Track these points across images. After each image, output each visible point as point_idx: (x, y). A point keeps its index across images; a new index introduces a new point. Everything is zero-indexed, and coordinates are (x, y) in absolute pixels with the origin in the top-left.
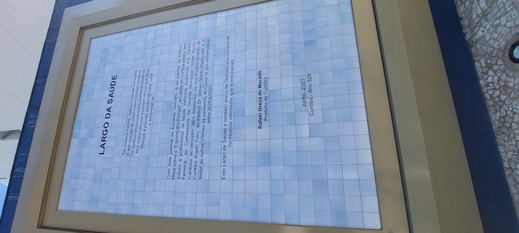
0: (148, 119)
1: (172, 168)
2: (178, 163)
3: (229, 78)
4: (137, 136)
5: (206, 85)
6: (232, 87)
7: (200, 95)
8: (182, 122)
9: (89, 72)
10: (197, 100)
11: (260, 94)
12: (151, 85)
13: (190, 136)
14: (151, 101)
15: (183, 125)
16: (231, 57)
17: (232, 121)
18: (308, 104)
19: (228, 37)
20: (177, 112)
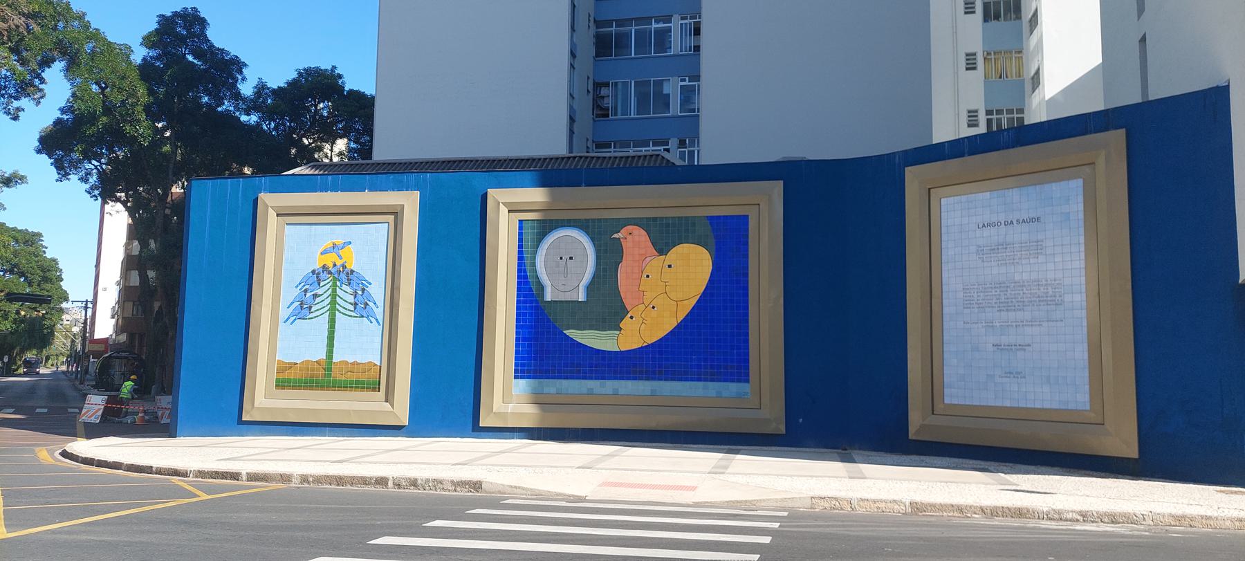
5: (1026, 306)
8: (998, 290)
10: (1014, 300)
11: (1015, 345)
15: (996, 291)
16: (1045, 324)
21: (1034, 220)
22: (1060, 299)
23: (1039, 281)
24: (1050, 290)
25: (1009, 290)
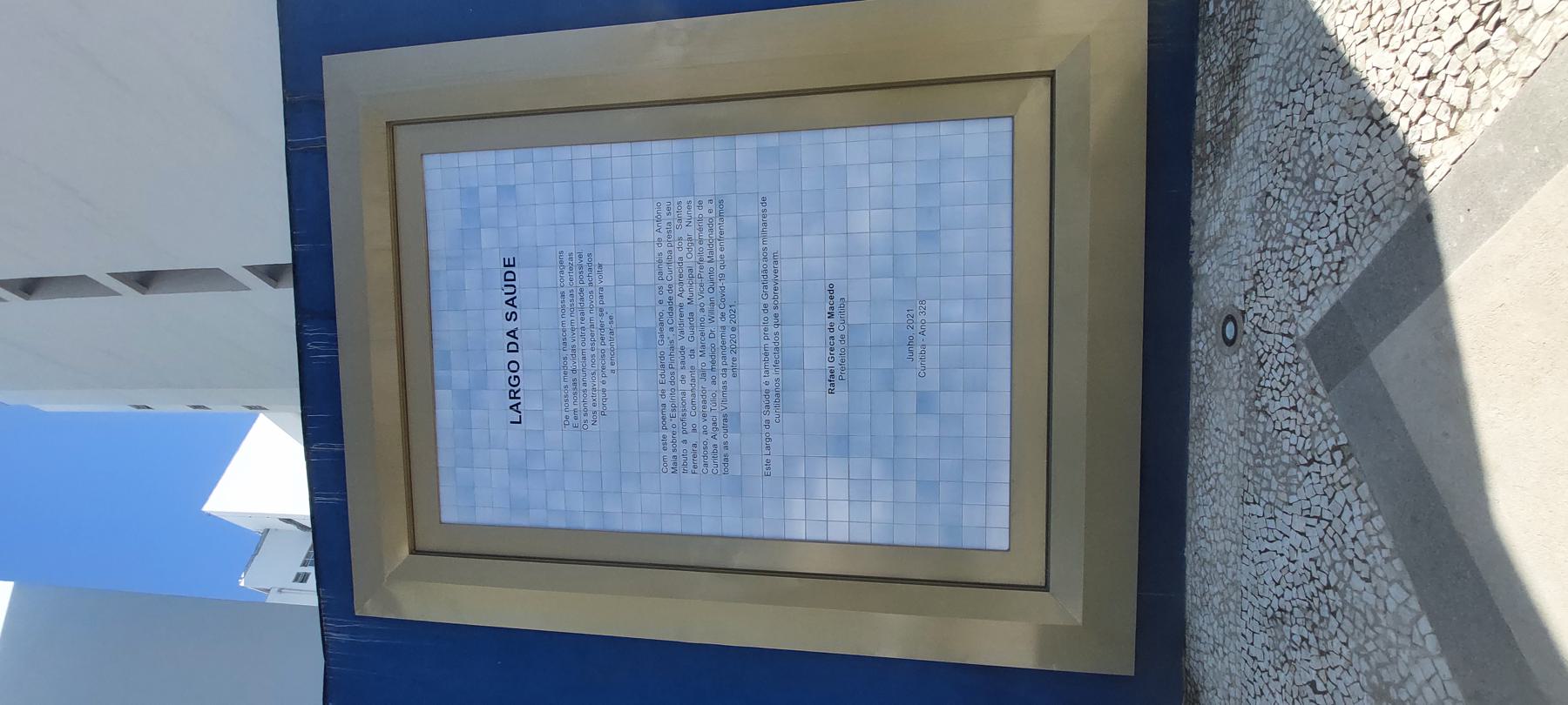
0: (608, 362)
1: (669, 454)
2: (681, 447)
3: (770, 290)
4: (589, 393)
6: (777, 311)
7: (711, 320)
9: (439, 241)
10: (707, 331)
11: (831, 329)
12: (601, 289)
13: (698, 400)
14: (607, 325)
15: (683, 377)
16: (773, 244)
17: (779, 376)
18: (917, 356)
19: (764, 199)
20: (667, 352)
21: (510, 276)
22: (707, 206)
23: (660, 262)
24: (683, 232)
25: (679, 344)
